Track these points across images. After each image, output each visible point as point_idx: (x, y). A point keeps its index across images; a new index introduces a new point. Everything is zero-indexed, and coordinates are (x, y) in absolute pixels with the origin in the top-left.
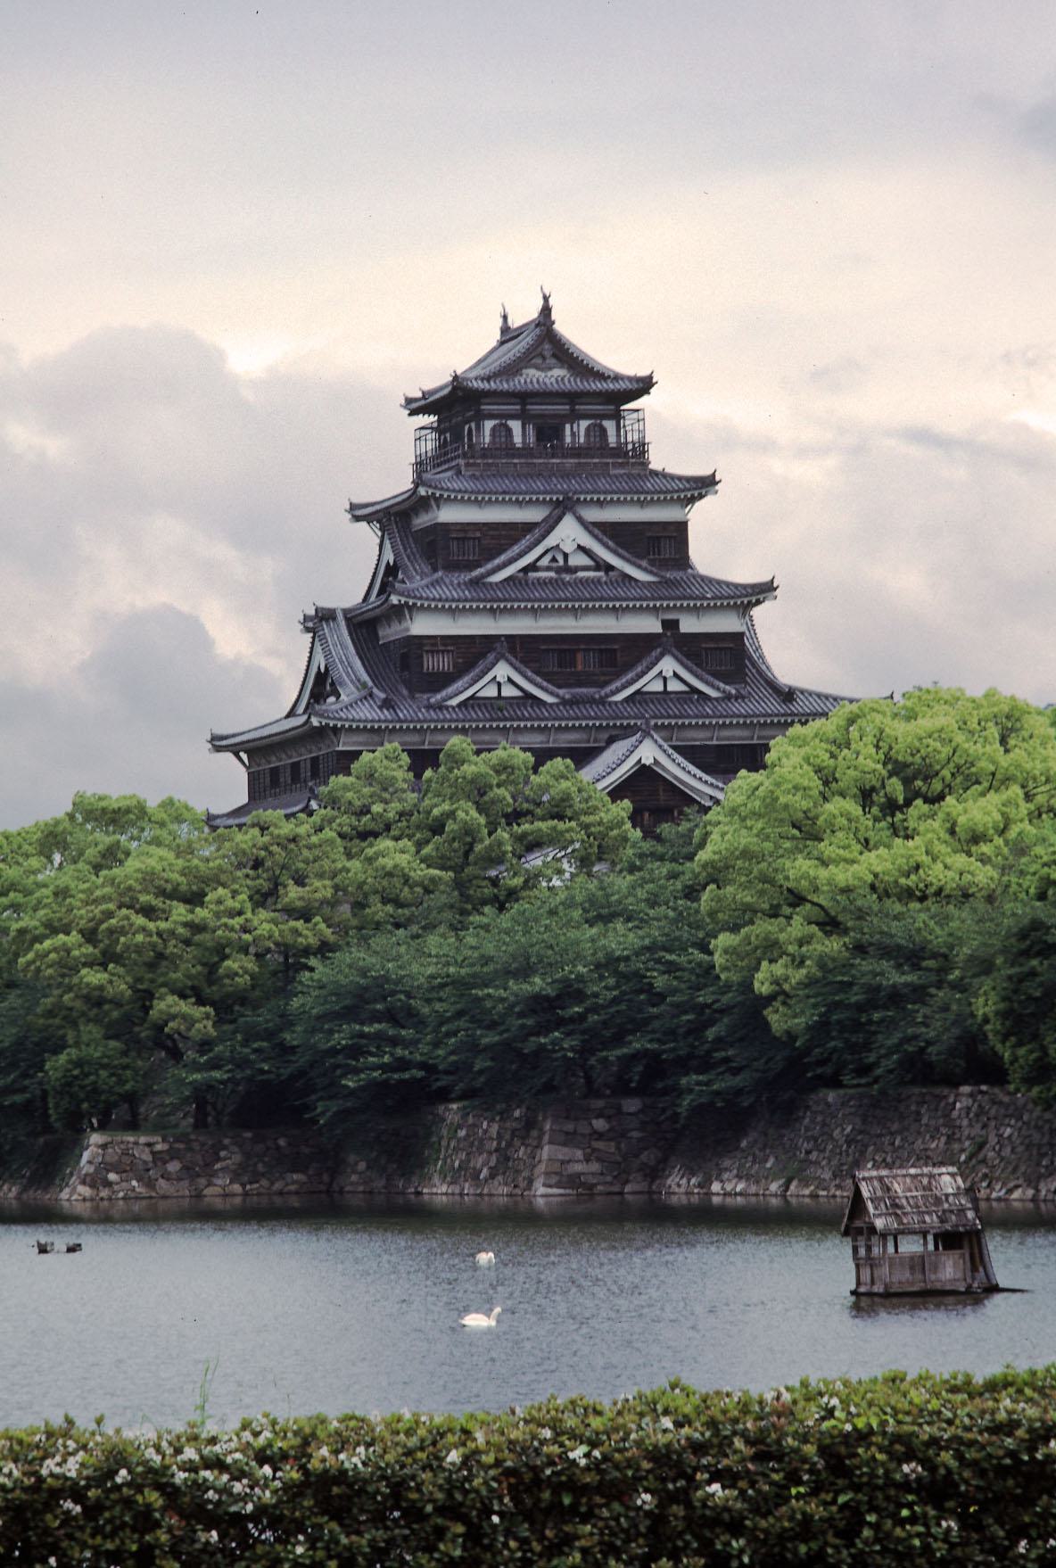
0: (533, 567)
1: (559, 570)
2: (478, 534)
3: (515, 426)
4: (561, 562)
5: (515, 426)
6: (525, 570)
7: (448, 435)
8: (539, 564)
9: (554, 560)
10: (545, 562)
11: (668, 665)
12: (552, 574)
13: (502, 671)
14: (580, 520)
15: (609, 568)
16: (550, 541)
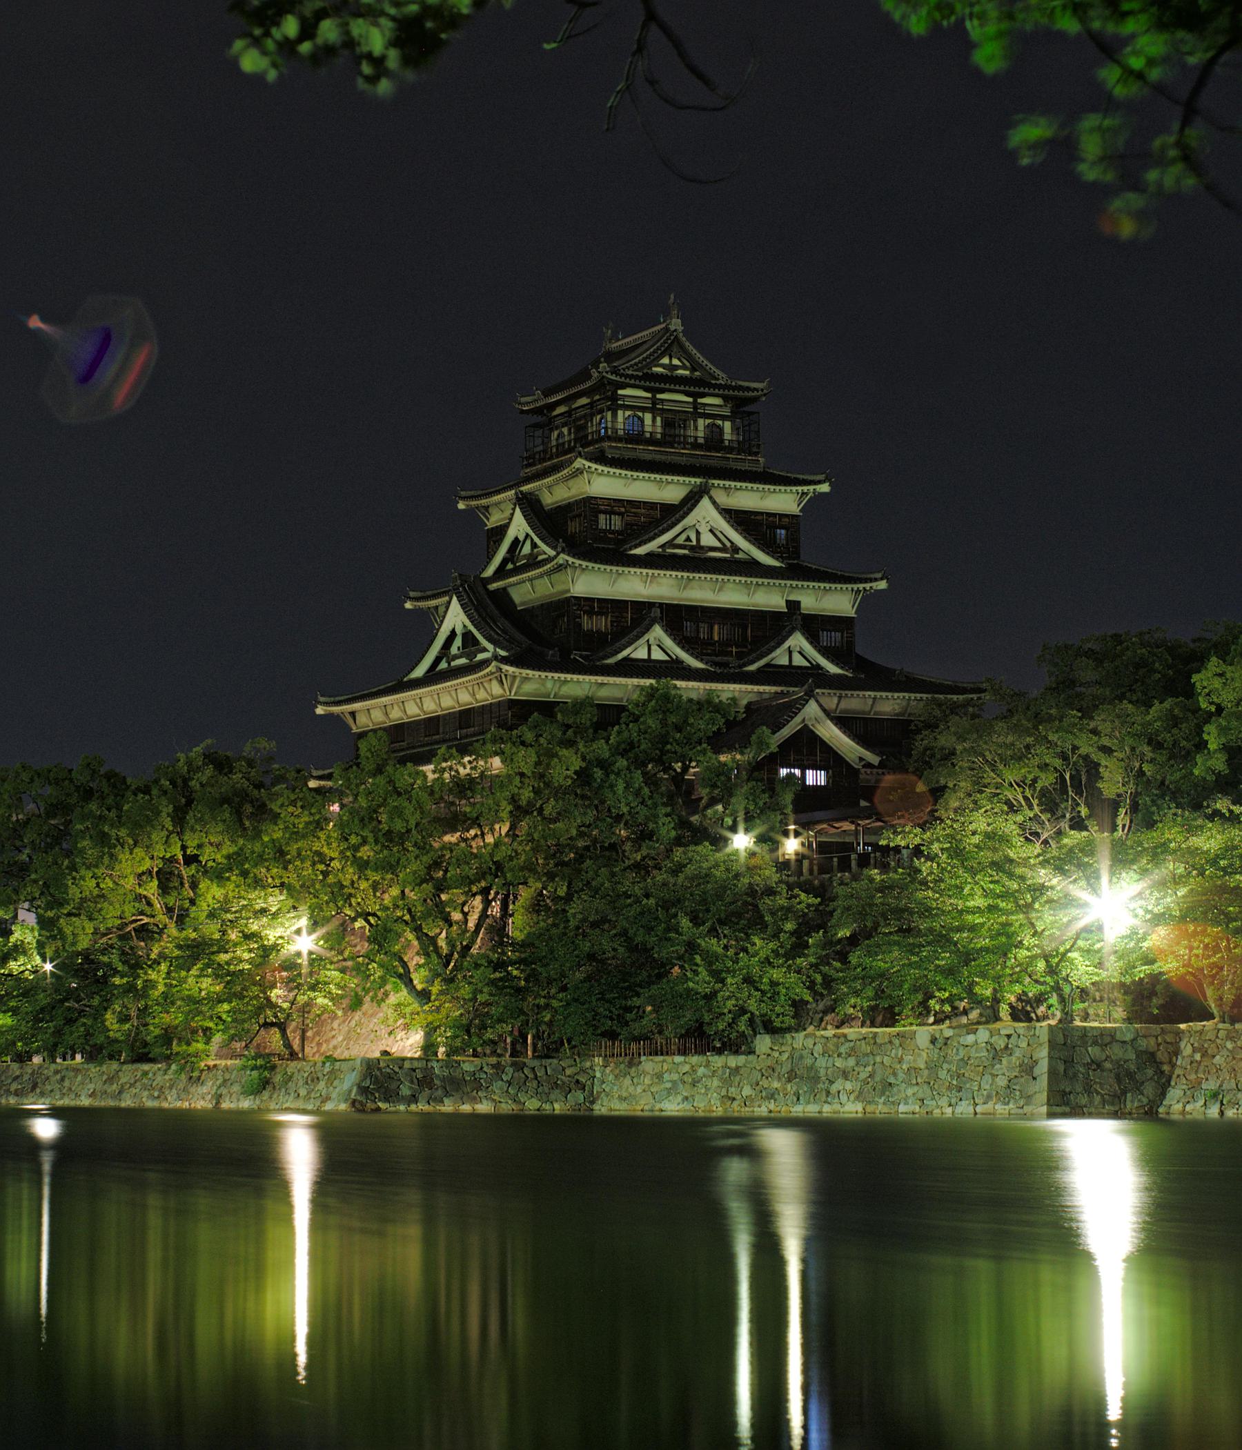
0: (671, 543)
1: (692, 548)
2: (623, 510)
3: (648, 418)
4: (694, 543)
5: (648, 418)
6: (662, 546)
7: (565, 430)
8: (676, 542)
9: (688, 539)
10: (680, 540)
11: (798, 641)
12: (686, 552)
13: (657, 632)
14: (714, 503)
15: (736, 549)
16: (688, 521)
